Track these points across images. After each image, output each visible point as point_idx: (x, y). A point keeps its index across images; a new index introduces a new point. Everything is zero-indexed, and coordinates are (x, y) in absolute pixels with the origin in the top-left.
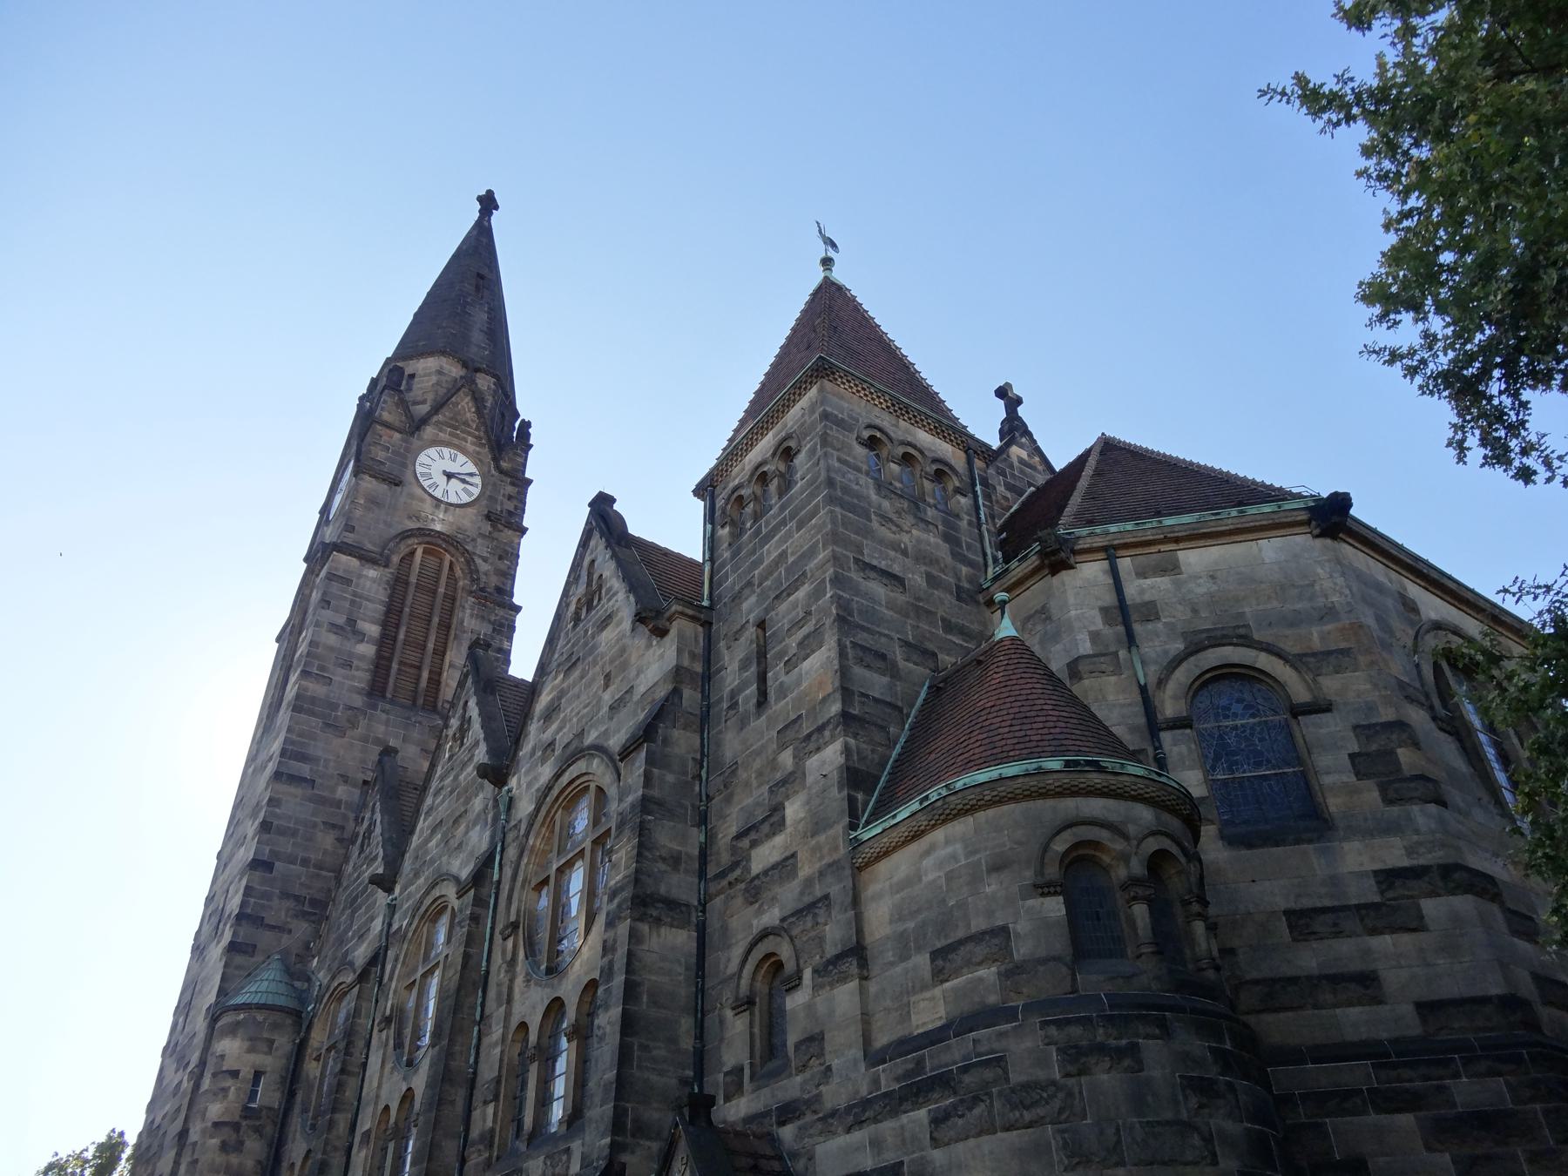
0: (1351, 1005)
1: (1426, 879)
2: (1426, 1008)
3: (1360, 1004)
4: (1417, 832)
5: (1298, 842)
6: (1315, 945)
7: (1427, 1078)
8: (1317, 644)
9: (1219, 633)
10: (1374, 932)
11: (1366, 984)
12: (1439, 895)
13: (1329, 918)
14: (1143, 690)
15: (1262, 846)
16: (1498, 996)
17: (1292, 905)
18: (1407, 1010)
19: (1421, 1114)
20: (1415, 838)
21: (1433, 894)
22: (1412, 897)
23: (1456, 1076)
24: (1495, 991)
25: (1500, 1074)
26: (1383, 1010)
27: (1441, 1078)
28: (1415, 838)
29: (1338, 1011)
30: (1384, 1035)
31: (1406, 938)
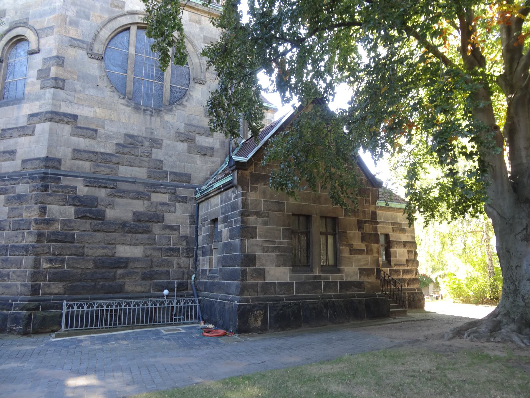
0: (7, 161)
1: (39, 117)
2: (24, 161)
3: (8, 160)
4: (45, 99)
5: (13, 105)
6: (5, 141)
7: (11, 184)
8: (45, 25)
9: (18, 22)
10: (20, 136)
11: (11, 153)
12: (41, 123)
13: (10, 131)
14: (70, 45)
15: (4, 106)
16: (44, 158)
17: (4, 128)
18: (20, 162)
19: (6, 195)
20: (44, 102)
21: (40, 122)
22: (34, 124)
23: (19, 183)
24: (43, 155)
25: (29, 183)
26: (13, 162)
27: (14, 184)
28: (44, 102)
29: (3, 163)
30: (11, 171)
31: (28, 138)
